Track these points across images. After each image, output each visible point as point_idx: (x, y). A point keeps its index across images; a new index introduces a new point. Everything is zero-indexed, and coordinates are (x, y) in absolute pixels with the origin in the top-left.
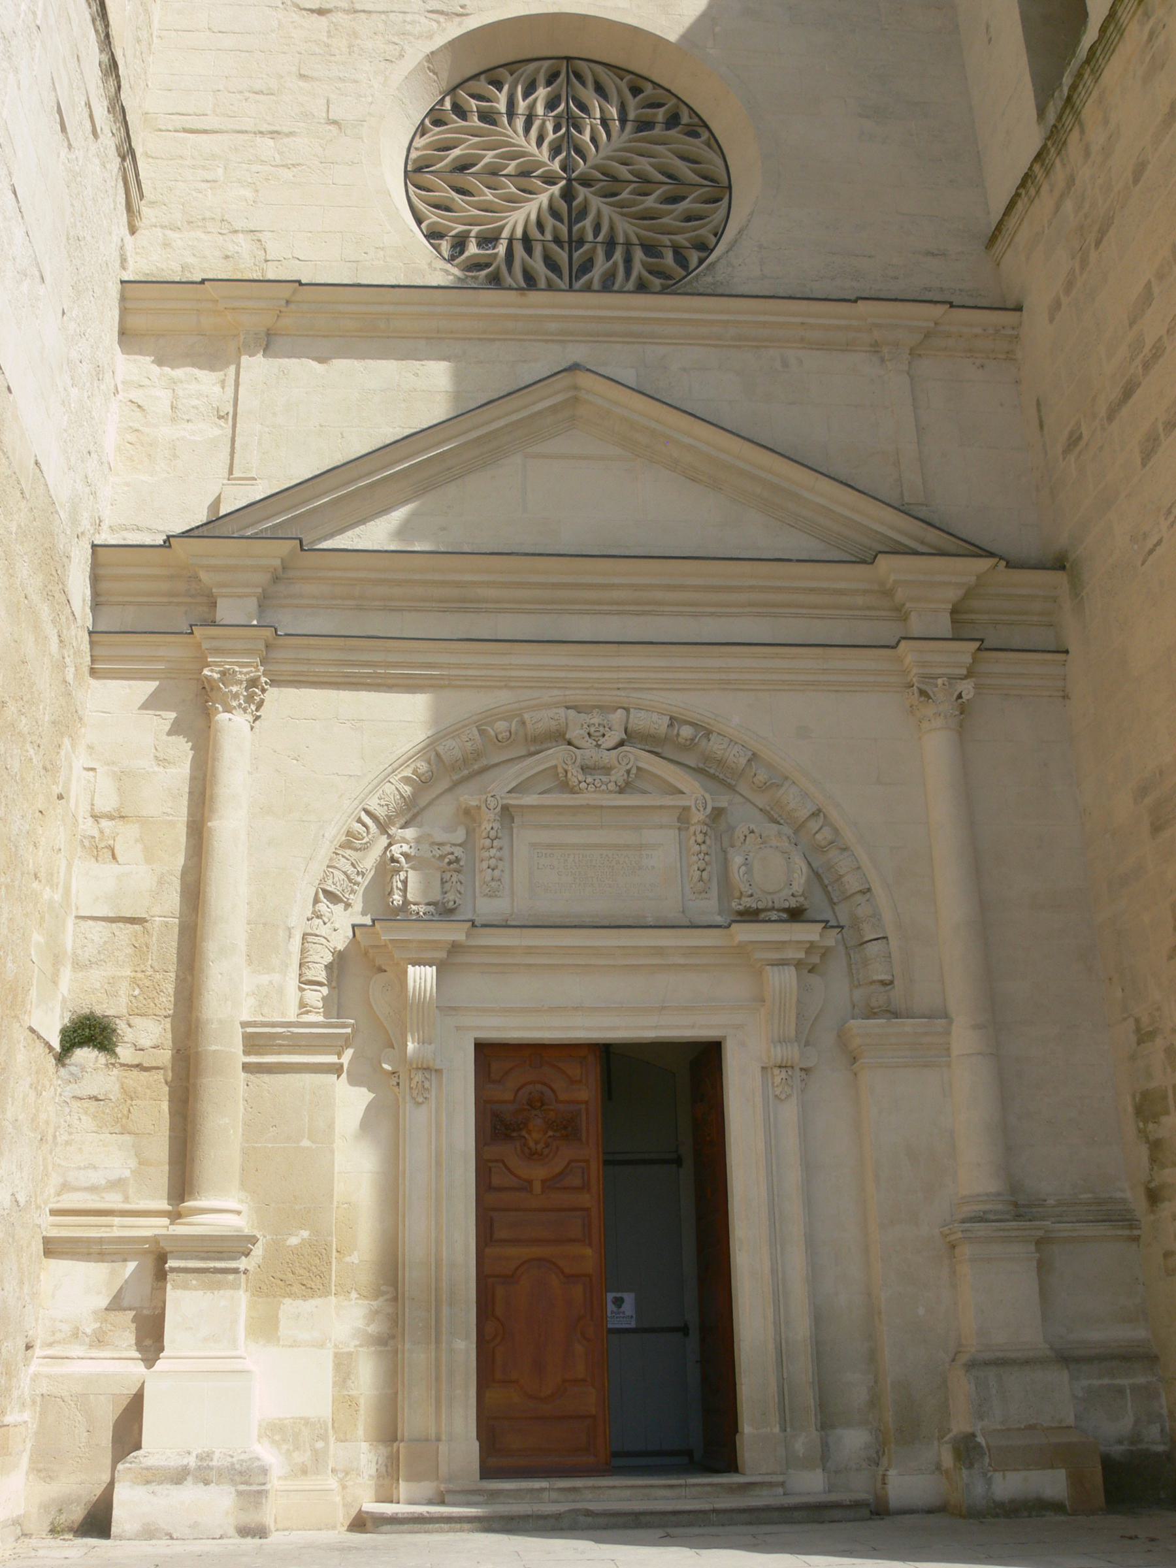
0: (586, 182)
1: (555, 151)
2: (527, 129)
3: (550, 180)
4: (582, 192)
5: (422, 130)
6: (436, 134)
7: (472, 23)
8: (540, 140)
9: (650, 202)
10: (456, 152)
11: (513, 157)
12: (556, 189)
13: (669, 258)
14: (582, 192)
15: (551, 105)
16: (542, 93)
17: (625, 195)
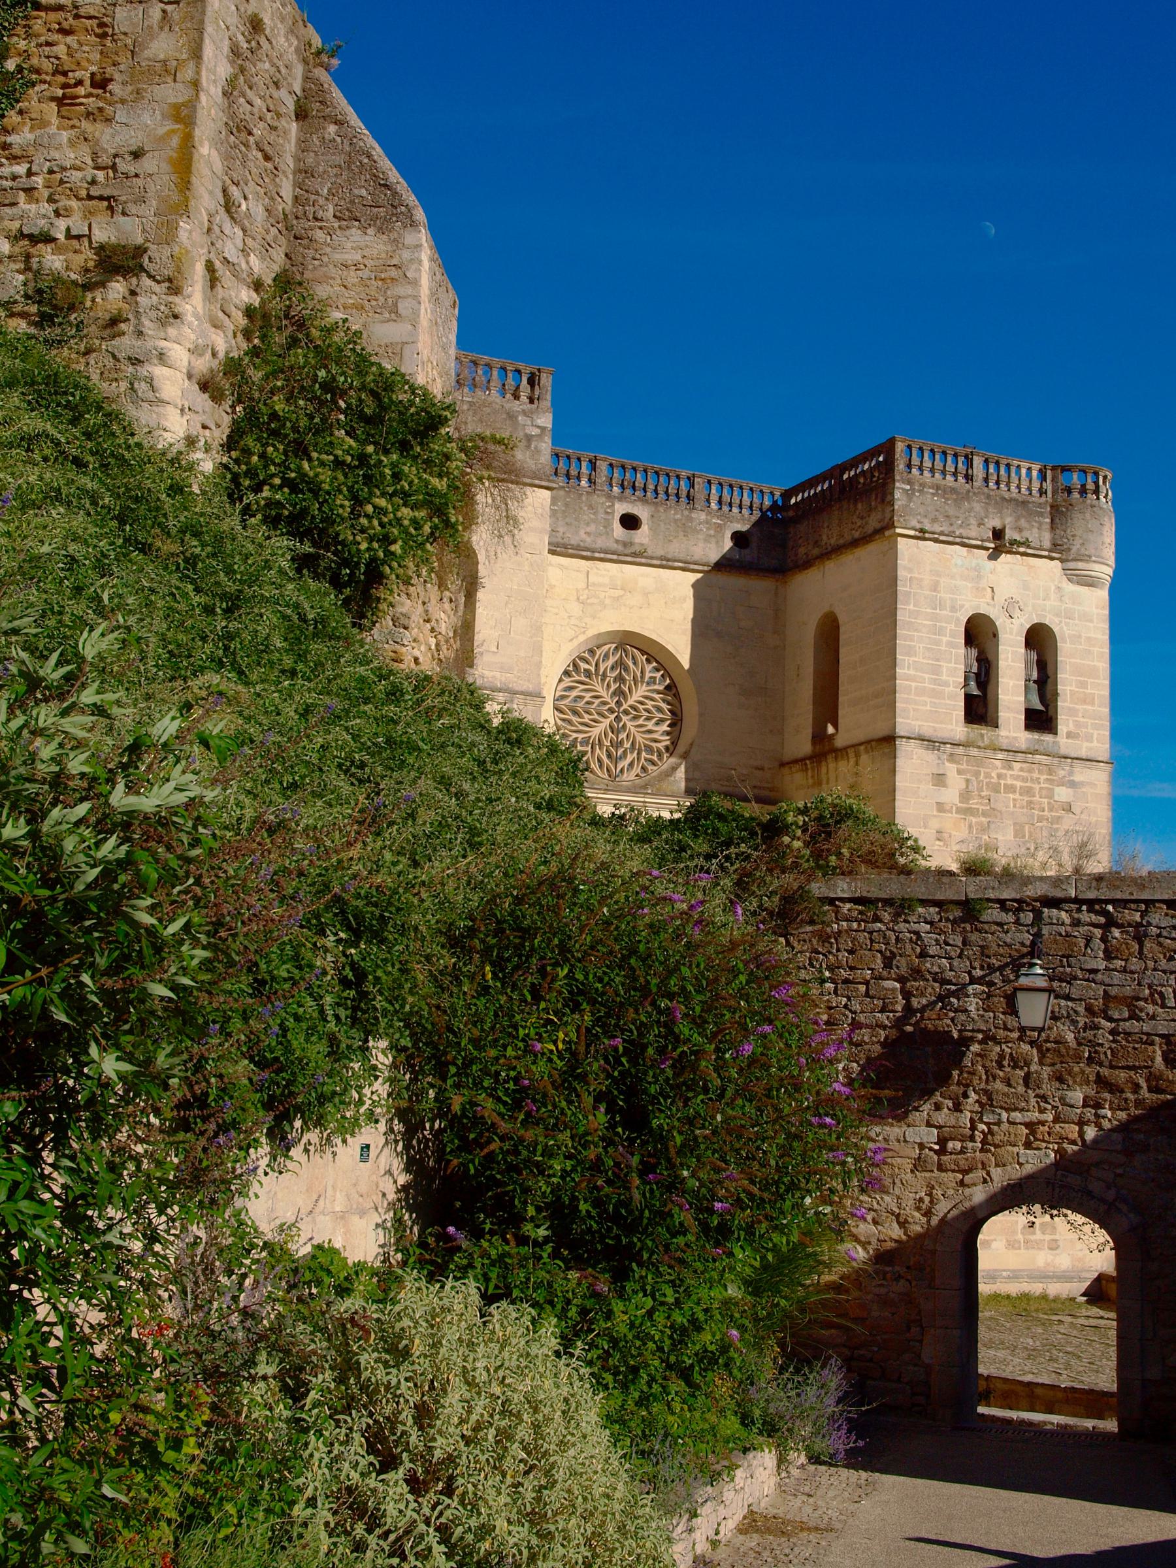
0: (626, 712)
1: (614, 694)
2: (603, 680)
3: (611, 711)
4: (624, 718)
5: (560, 680)
6: (567, 682)
7: (591, 632)
8: (608, 686)
9: (650, 725)
10: (574, 693)
11: (597, 697)
12: (613, 716)
13: (655, 758)
14: (624, 718)
15: (612, 668)
16: (612, 660)
17: (641, 722)
